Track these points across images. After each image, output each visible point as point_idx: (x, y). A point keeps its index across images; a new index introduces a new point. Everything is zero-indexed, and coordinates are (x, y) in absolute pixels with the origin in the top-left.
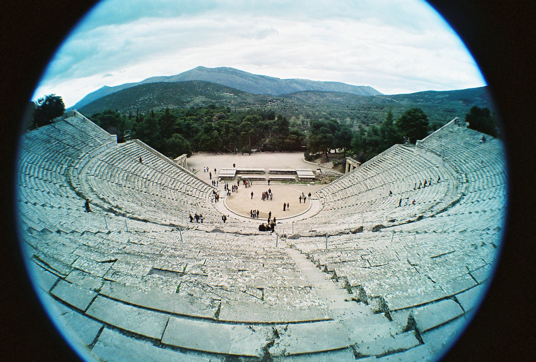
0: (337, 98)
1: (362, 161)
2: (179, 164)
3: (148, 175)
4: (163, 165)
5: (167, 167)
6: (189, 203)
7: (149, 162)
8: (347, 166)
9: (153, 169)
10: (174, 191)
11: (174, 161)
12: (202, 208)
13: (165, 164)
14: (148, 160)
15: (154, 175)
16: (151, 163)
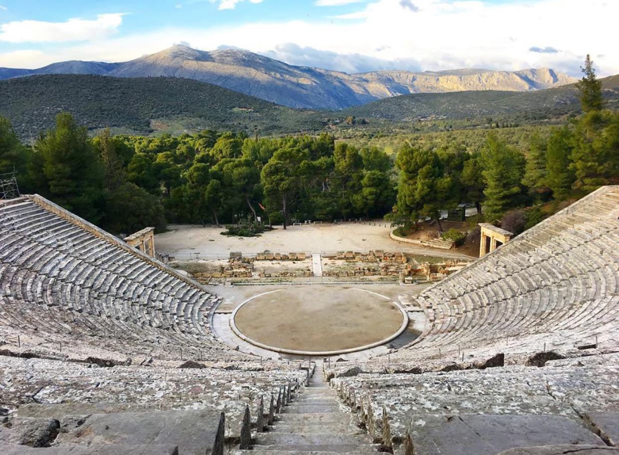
0: (468, 106)
1: (516, 229)
2: (138, 248)
3: (61, 270)
4: (100, 249)
5: (109, 253)
6: (154, 325)
7: (67, 243)
8: (483, 242)
9: (76, 257)
10: (121, 301)
11: (126, 241)
12: (183, 335)
13: (104, 247)
14: (63, 239)
15: (76, 269)
16: (71, 244)
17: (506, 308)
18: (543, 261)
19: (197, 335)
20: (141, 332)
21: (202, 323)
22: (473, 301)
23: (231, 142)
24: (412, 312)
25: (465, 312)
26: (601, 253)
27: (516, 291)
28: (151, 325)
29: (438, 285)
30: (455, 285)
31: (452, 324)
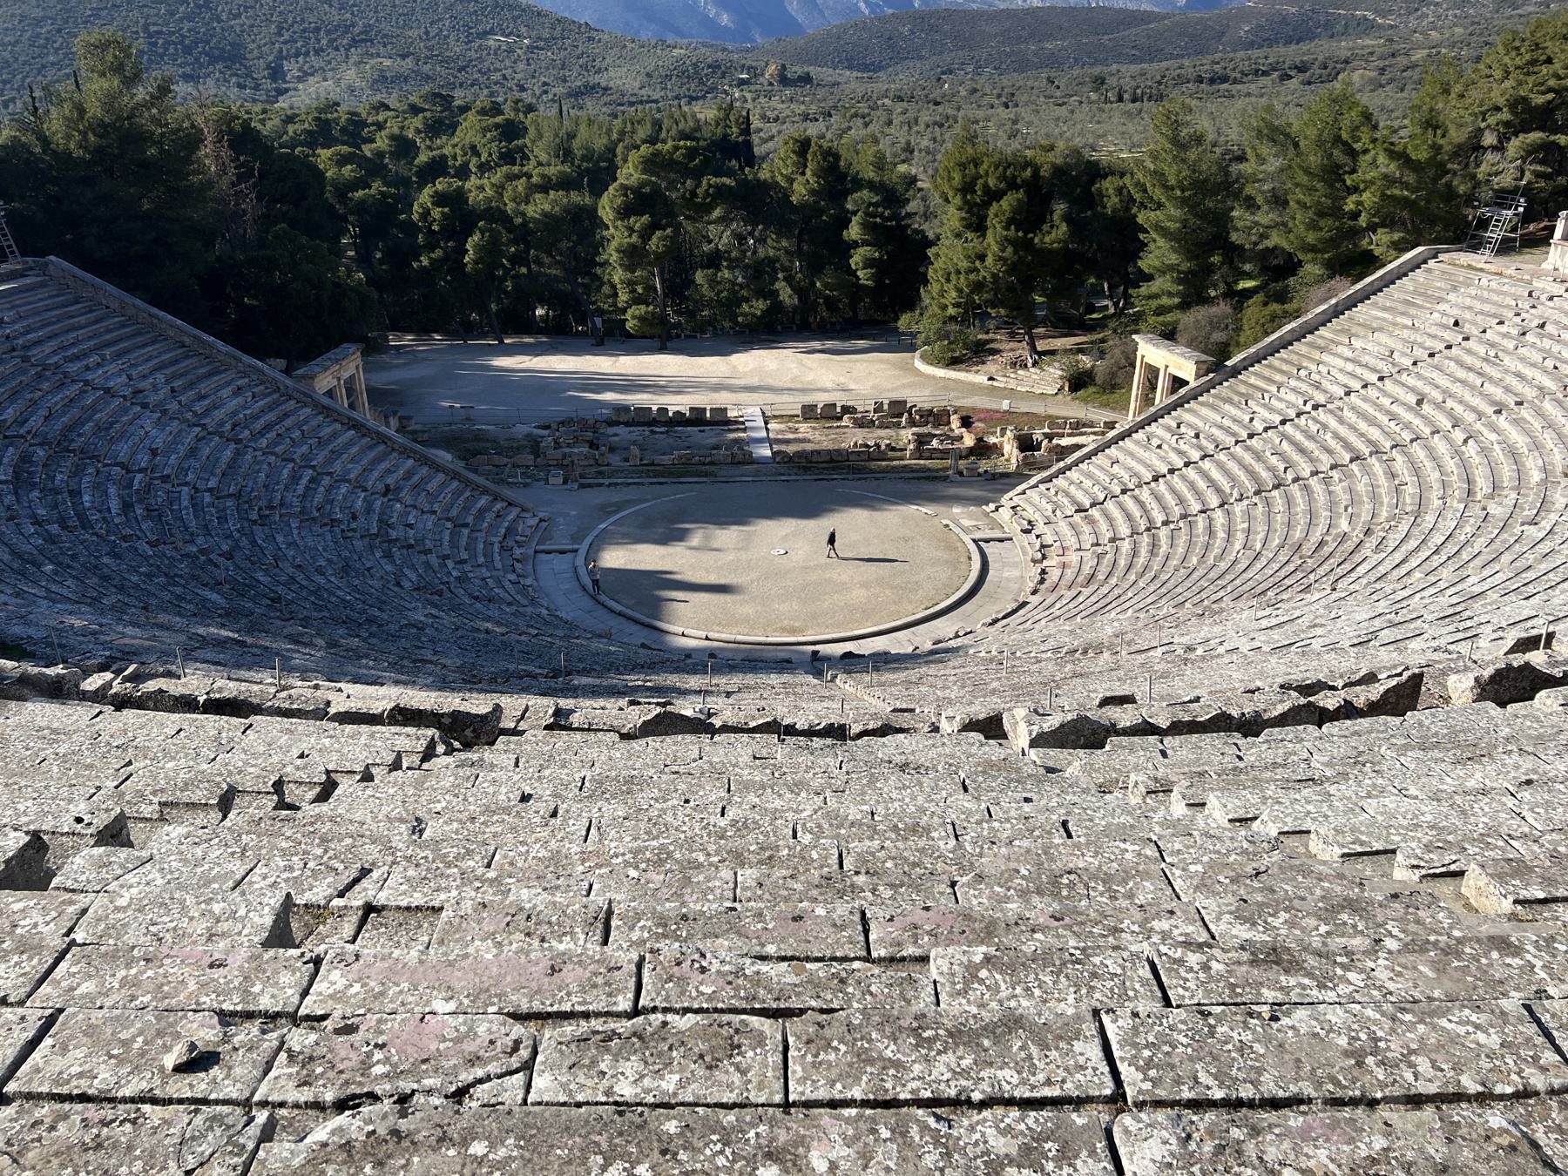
6: (407, 584)
17: (1211, 532)
18: (1283, 422)
19: (510, 604)
20: (384, 602)
21: (513, 577)
22: (1129, 517)
23: (497, 126)
24: (987, 541)
25: (1112, 540)
26: (1419, 402)
27: (1228, 491)
28: (398, 584)
29: (1042, 481)
30: (1080, 482)
31: (1087, 570)
